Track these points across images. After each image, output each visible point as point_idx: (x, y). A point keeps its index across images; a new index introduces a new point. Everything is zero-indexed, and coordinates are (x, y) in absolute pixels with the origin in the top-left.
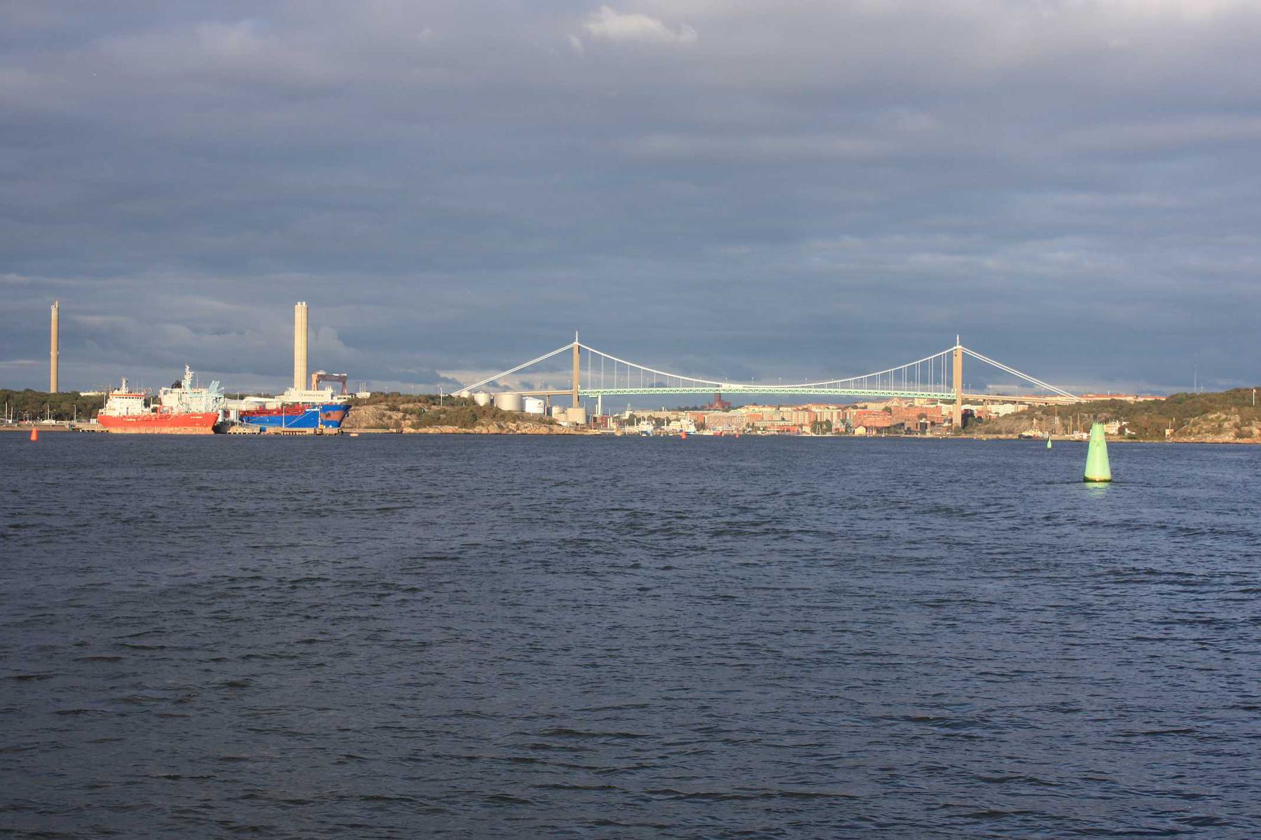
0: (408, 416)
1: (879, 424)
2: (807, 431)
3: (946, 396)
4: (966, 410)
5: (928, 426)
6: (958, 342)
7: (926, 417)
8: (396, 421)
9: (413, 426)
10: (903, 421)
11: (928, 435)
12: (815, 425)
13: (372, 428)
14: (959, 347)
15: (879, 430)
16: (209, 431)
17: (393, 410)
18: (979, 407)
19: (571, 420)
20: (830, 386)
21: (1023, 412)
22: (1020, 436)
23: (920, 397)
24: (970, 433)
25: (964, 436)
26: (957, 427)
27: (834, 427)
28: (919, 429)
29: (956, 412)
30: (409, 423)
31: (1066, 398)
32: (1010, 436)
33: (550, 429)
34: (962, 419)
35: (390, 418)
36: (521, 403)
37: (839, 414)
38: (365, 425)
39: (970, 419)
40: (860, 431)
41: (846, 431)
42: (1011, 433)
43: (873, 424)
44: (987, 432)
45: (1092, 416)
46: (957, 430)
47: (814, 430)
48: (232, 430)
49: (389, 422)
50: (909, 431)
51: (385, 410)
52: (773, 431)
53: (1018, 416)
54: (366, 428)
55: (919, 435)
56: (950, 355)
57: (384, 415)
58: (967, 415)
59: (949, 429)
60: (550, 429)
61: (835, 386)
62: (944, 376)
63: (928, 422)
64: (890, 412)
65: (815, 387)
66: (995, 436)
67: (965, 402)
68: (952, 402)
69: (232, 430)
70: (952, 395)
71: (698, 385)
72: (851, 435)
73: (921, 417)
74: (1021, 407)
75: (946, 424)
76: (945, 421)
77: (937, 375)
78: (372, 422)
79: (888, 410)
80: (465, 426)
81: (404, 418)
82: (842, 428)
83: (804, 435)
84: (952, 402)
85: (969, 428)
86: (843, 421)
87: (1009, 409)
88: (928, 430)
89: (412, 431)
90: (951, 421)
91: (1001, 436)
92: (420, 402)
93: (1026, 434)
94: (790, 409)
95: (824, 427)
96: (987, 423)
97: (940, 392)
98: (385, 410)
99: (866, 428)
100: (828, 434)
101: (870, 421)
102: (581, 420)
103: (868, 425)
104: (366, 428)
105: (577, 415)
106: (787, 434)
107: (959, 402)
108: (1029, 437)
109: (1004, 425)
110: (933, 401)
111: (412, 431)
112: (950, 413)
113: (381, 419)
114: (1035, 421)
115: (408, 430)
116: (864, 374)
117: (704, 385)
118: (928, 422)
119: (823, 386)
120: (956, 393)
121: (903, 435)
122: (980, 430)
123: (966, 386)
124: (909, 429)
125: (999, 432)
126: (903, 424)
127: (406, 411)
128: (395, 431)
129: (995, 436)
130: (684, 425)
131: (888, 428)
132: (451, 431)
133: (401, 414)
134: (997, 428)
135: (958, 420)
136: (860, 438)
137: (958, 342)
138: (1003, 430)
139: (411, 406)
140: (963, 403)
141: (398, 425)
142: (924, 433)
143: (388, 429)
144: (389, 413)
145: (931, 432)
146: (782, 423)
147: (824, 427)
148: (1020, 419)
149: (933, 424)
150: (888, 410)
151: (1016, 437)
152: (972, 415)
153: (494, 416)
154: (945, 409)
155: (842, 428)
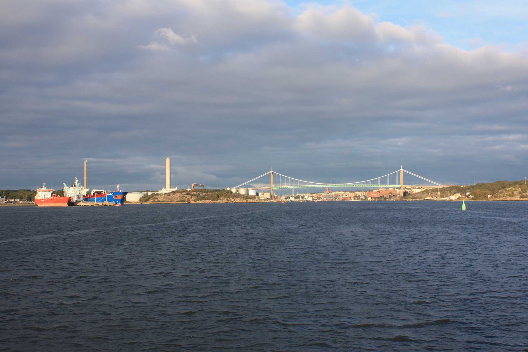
0: (193, 197)
1: (376, 196)
2: (352, 199)
3: (398, 186)
4: (406, 191)
7: (391, 194)
8: (188, 199)
9: (194, 201)
10: (383, 195)
11: (392, 200)
12: (356, 197)
13: (179, 201)
14: (402, 169)
15: (375, 198)
16: (66, 205)
17: (188, 195)
18: (410, 190)
19: (265, 197)
20: (358, 184)
21: (424, 191)
22: (424, 199)
23: (391, 187)
24: (406, 199)
25: (404, 200)
26: (402, 196)
27: (361, 198)
29: (402, 192)
30: (193, 199)
31: (441, 186)
32: (420, 199)
33: (247, 200)
35: (186, 197)
36: (248, 192)
37: (364, 193)
38: (176, 200)
39: (406, 194)
40: (369, 199)
41: (365, 199)
42: (421, 198)
43: (374, 196)
44: (412, 198)
46: (401, 198)
47: (354, 199)
48: (79, 204)
49: (185, 199)
50: (385, 198)
51: (185, 195)
52: (341, 199)
53: (423, 192)
54: (176, 201)
55: (389, 200)
57: (184, 197)
58: (405, 193)
59: (399, 197)
60: (247, 200)
61: (360, 184)
63: (392, 195)
64: (380, 192)
65: (353, 184)
66: (415, 200)
67: (405, 188)
68: (399, 188)
69: (79, 204)
71: (313, 184)
72: (366, 200)
73: (389, 194)
74: (423, 190)
75: (398, 196)
77: (395, 180)
78: (179, 199)
79: (379, 192)
80: (214, 200)
81: (191, 198)
82: (364, 198)
83: (351, 200)
84: (399, 188)
85: (406, 197)
86: (364, 196)
87: (420, 190)
88: (392, 198)
89: (194, 202)
90: (400, 194)
91: (417, 200)
92: (199, 191)
93: (426, 198)
94: (349, 192)
95: (358, 198)
96: (412, 195)
97: (396, 184)
98: (185, 195)
99: (371, 197)
100: (359, 200)
101: (373, 195)
102: (269, 197)
103: (372, 196)
104: (176, 201)
105: (267, 195)
106: (345, 200)
107: (402, 188)
108: (427, 200)
109: (418, 196)
110: (394, 188)
111: (194, 202)
112: (400, 192)
113: (182, 198)
114: (429, 194)
115: (192, 202)
117: (315, 184)
118: (392, 195)
121: (383, 200)
124: (385, 198)
125: (417, 198)
126: (383, 196)
127: (192, 195)
128: (187, 202)
129: (415, 200)
130: (309, 198)
131: (379, 197)
132: (208, 202)
133: (190, 196)
134: (416, 197)
135: (402, 194)
136: (369, 201)
138: (418, 197)
139: (195, 193)
140: (404, 189)
141: (189, 200)
142: (391, 199)
143: (185, 201)
144: (186, 196)
145: (393, 198)
146: (345, 197)
147: (358, 198)
148: (424, 193)
149: (394, 196)
150: (379, 192)
151: (422, 200)
152: (407, 193)
153: (226, 196)
154: (398, 191)
155: (364, 198)
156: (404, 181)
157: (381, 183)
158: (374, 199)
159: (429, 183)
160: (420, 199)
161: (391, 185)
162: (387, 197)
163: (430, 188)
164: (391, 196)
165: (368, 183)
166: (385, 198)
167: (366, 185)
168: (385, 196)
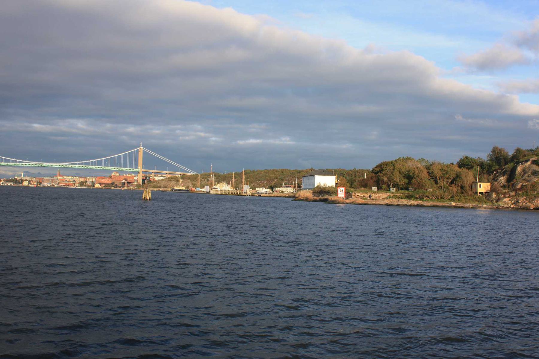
5: (126, 184)
6: (141, 145)
11: (126, 188)
14: (142, 147)
20: (79, 164)
28: (121, 185)
29: (139, 178)
34: (142, 181)
44: (154, 187)
45: (206, 180)
50: (116, 186)
56: (137, 151)
59: (136, 185)
61: (82, 164)
62: (134, 162)
63: (126, 182)
65: (72, 164)
71: (13, 161)
75: (136, 183)
76: (135, 182)
77: (132, 161)
88: (126, 185)
91: (160, 189)
96: (154, 182)
107: (141, 173)
109: (162, 184)
112: (137, 178)
117: (16, 162)
119: (76, 164)
120: (140, 169)
122: (150, 186)
123: (145, 165)
125: (160, 187)
129: (158, 189)
134: (159, 185)
135: (140, 182)
137: (141, 145)
142: (124, 187)
145: (128, 186)
157: (112, 165)
159: (176, 169)
160: (166, 189)
161: (125, 168)
162: (118, 184)
163: (178, 174)
164: (125, 183)
165: (93, 164)
168: (116, 183)
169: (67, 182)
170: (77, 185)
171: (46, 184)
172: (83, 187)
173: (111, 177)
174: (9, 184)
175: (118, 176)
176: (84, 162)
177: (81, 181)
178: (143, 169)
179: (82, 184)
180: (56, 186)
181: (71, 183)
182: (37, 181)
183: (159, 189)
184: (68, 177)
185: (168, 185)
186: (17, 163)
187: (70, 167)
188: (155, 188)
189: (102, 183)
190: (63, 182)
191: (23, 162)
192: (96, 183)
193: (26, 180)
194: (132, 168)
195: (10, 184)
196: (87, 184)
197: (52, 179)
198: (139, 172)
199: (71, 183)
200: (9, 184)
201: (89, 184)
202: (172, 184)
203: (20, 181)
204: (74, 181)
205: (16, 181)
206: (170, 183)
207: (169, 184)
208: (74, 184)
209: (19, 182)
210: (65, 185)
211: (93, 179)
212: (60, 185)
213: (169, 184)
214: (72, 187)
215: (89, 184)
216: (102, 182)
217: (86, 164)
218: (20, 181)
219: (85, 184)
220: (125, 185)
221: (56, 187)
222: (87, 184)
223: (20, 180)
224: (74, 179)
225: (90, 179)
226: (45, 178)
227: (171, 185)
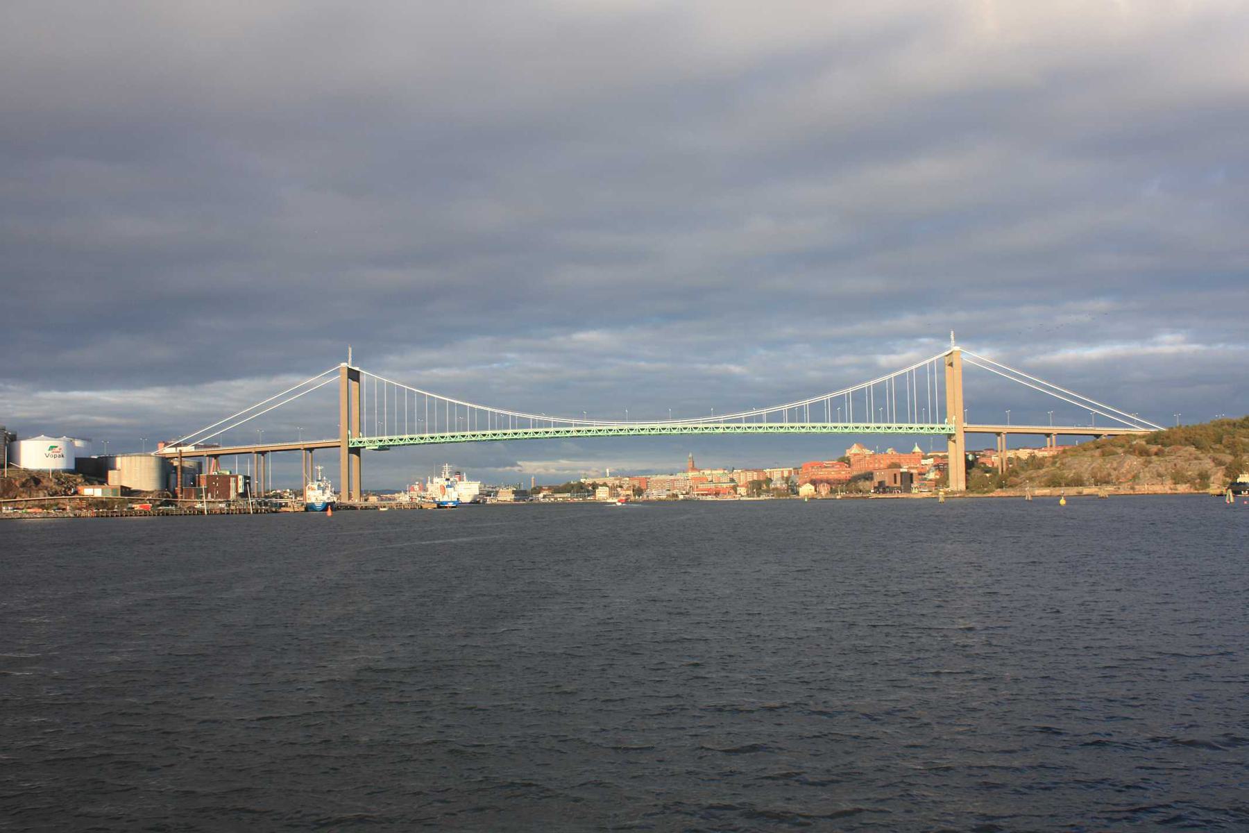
20: (748, 420)
28: (898, 484)
40: (806, 490)
50: (881, 487)
61: (759, 419)
70: (947, 426)
88: (915, 484)
107: (960, 438)
116: (804, 398)
117: (548, 424)
124: (881, 483)
142: (908, 489)
156: (964, 409)
158: (824, 490)
161: (905, 425)
162: (888, 482)
164: (912, 474)
166: (881, 483)
167: (786, 426)
169: (712, 486)
170: (742, 491)
171: (654, 494)
172: (762, 498)
173: (846, 461)
174: (560, 497)
175: (871, 456)
176: (786, 407)
177: (755, 478)
178: (965, 425)
179: (756, 486)
180: (681, 497)
181: (725, 485)
182: (634, 486)
183: (1080, 489)
184: (714, 472)
185: (1114, 473)
186: (552, 429)
187: (722, 431)
188: (1060, 485)
189: (821, 481)
190: (701, 486)
191: (570, 425)
192: (797, 480)
193: (605, 485)
194: (885, 422)
195: (563, 498)
196: (772, 486)
197: (672, 477)
198: (950, 436)
199: (725, 485)
200: (560, 497)
201: (778, 483)
202: (1126, 466)
203: (590, 488)
204: (732, 480)
205: (581, 488)
206: (1121, 464)
207: (1115, 469)
208: (735, 488)
209: (588, 491)
210: (707, 495)
211: (782, 472)
212: (694, 495)
213: (1115, 469)
214: (729, 498)
215: (778, 483)
216: (818, 477)
217: (773, 418)
218: (590, 488)
219: (764, 487)
220: (912, 482)
221: (682, 500)
222: (772, 486)
223: (590, 485)
224: (731, 476)
225: (777, 475)
226: (654, 478)
227: (1123, 470)
